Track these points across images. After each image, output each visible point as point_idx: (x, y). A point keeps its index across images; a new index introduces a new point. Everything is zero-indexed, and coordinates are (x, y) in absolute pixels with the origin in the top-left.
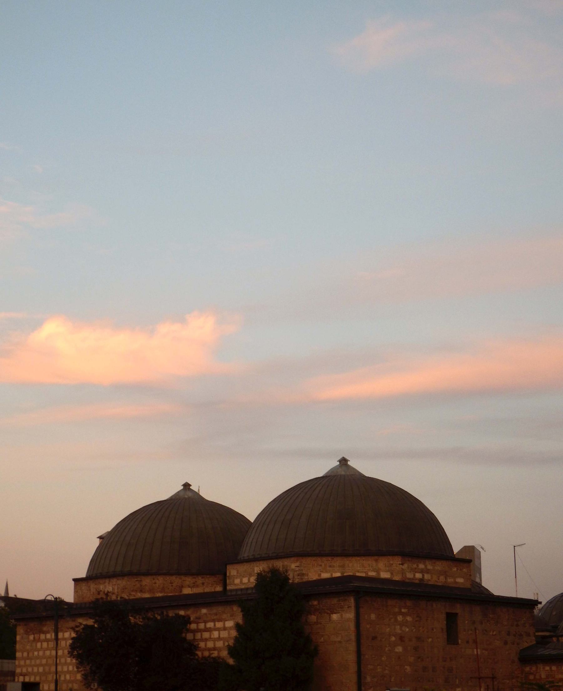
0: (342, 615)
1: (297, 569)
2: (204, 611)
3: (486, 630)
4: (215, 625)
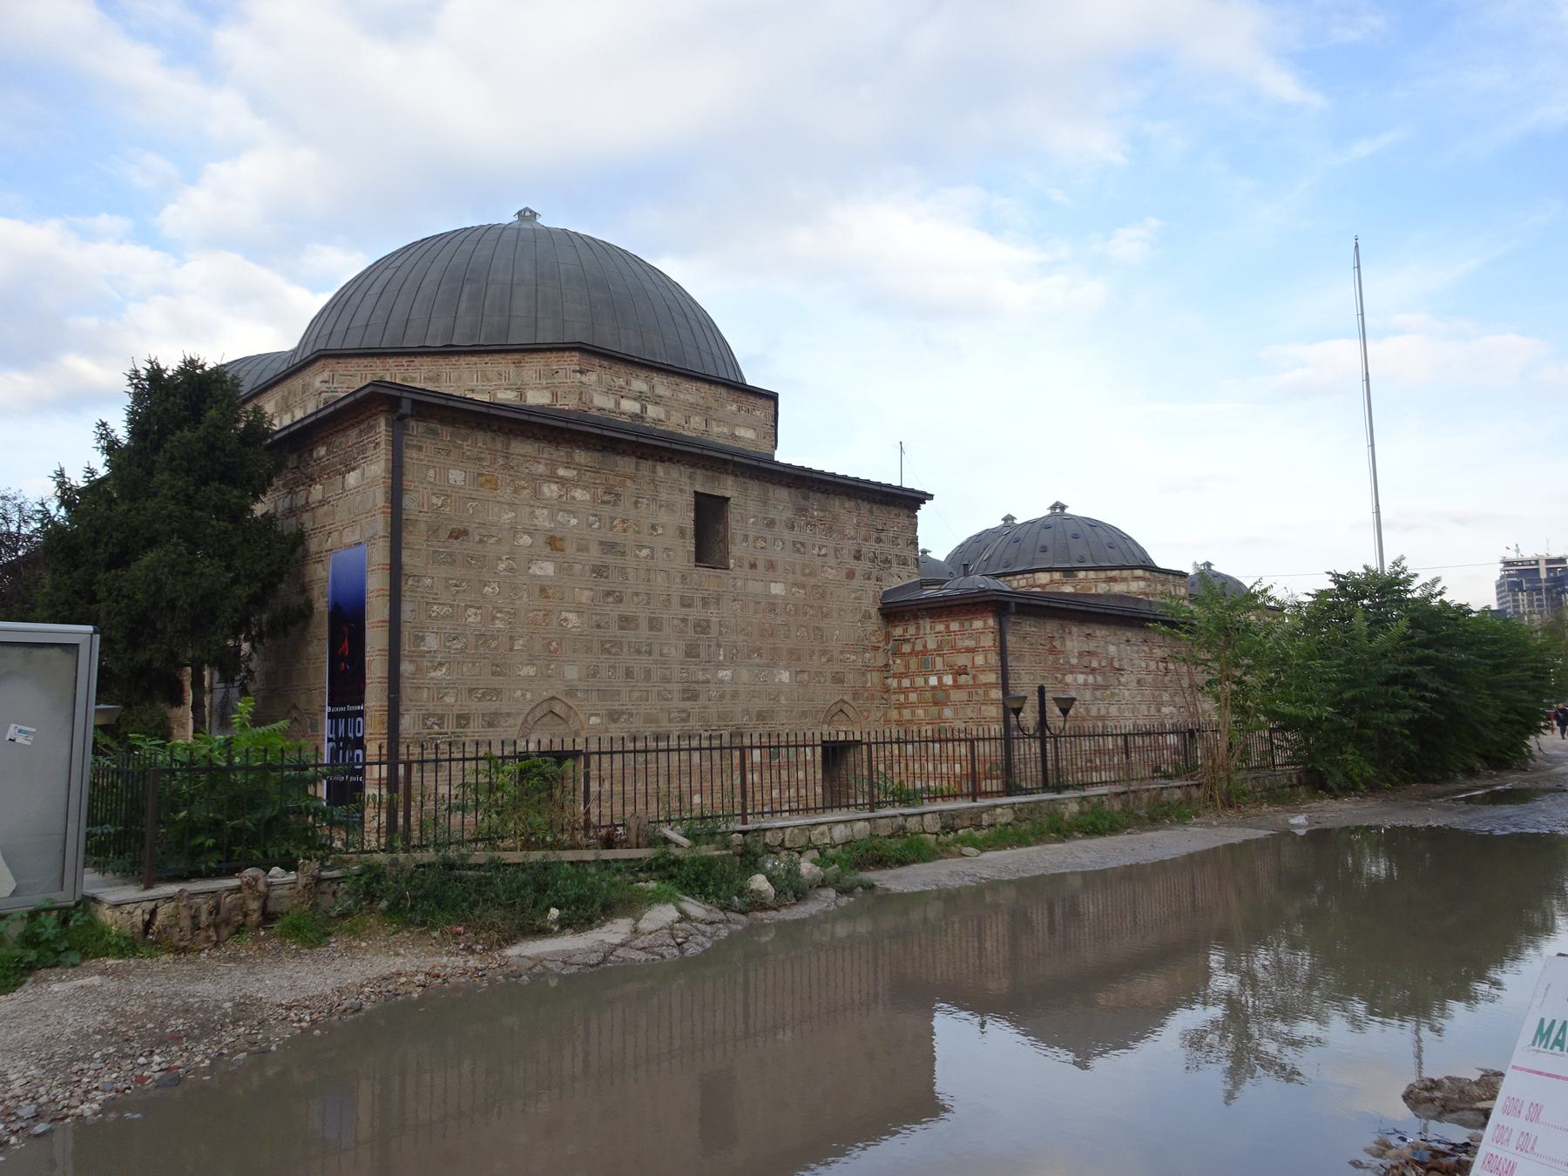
3: (802, 544)
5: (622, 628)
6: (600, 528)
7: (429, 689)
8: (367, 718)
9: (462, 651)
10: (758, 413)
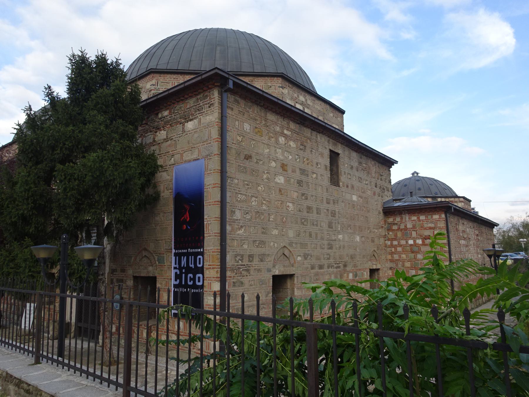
0: (200, 122)
1: (153, 87)
3: (361, 178)
5: (308, 212)
6: (299, 162)
7: (237, 240)
8: (205, 256)
9: (250, 220)
10: (339, 119)
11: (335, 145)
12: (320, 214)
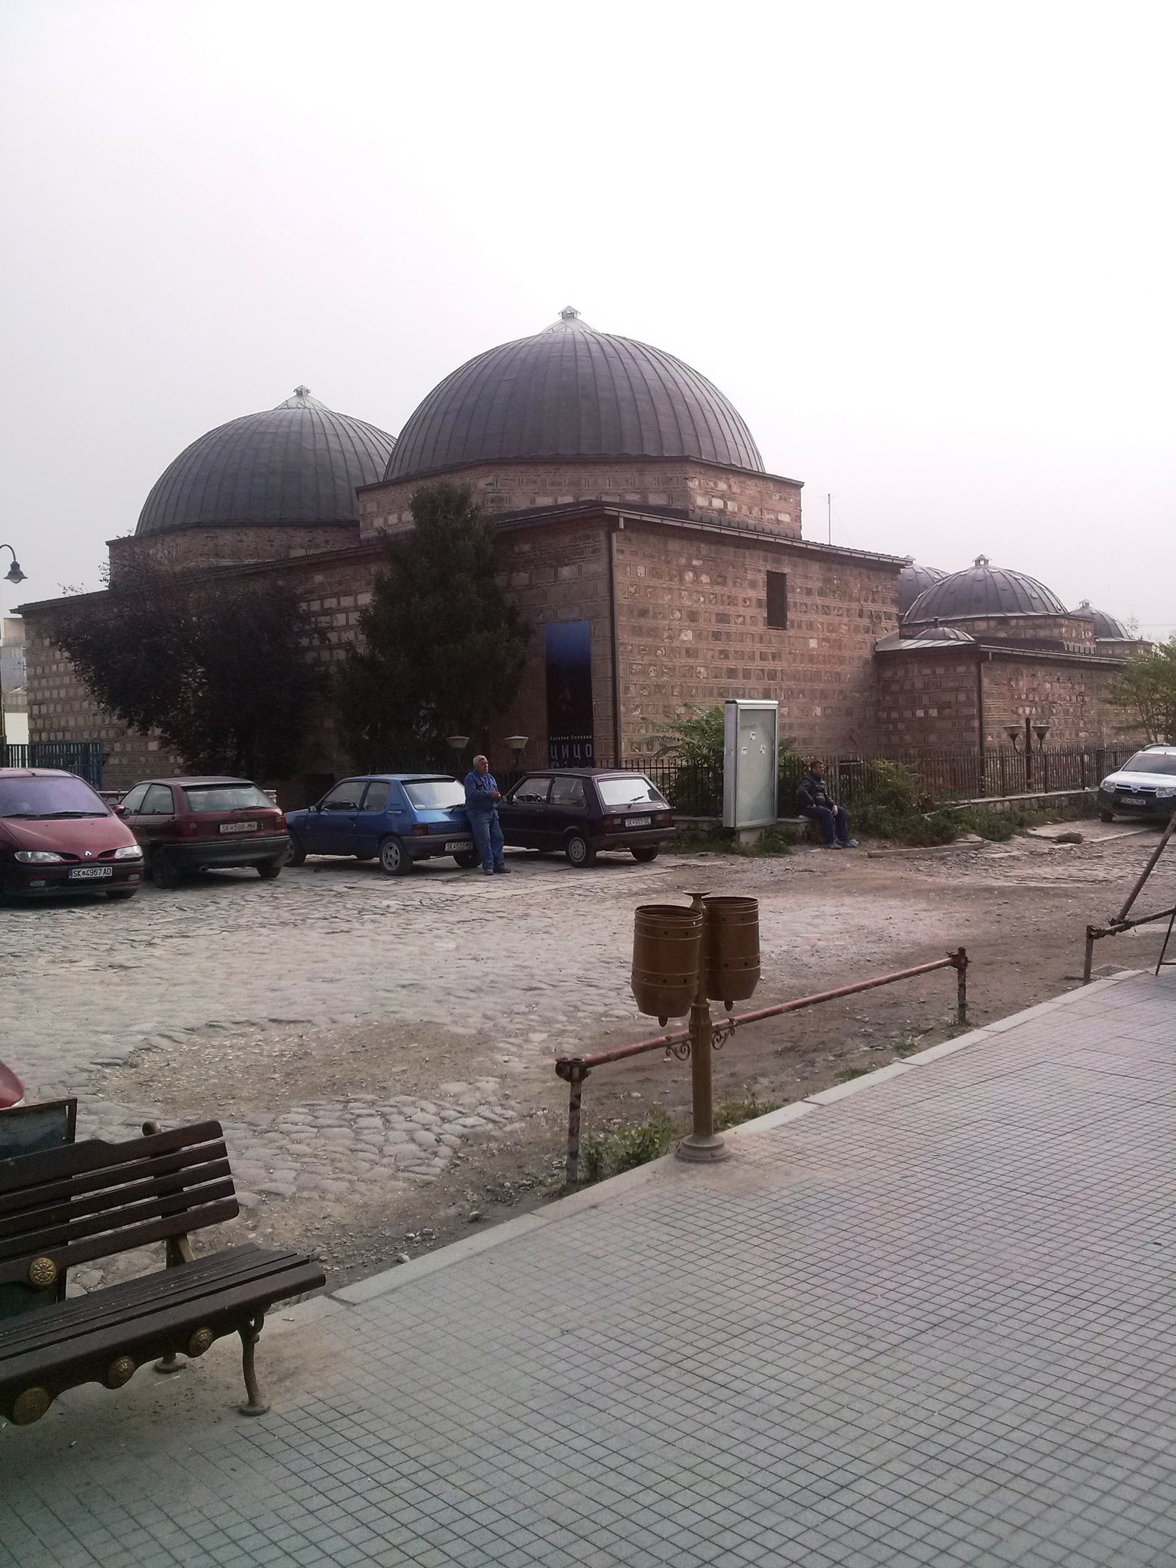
1: (490, 489)
2: (319, 578)
4: (339, 603)
8: (596, 744)
11: (777, 561)
12: (749, 678)
